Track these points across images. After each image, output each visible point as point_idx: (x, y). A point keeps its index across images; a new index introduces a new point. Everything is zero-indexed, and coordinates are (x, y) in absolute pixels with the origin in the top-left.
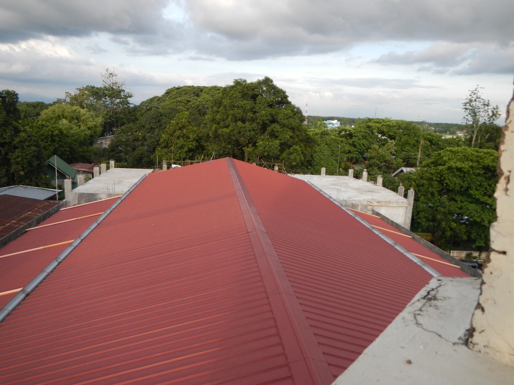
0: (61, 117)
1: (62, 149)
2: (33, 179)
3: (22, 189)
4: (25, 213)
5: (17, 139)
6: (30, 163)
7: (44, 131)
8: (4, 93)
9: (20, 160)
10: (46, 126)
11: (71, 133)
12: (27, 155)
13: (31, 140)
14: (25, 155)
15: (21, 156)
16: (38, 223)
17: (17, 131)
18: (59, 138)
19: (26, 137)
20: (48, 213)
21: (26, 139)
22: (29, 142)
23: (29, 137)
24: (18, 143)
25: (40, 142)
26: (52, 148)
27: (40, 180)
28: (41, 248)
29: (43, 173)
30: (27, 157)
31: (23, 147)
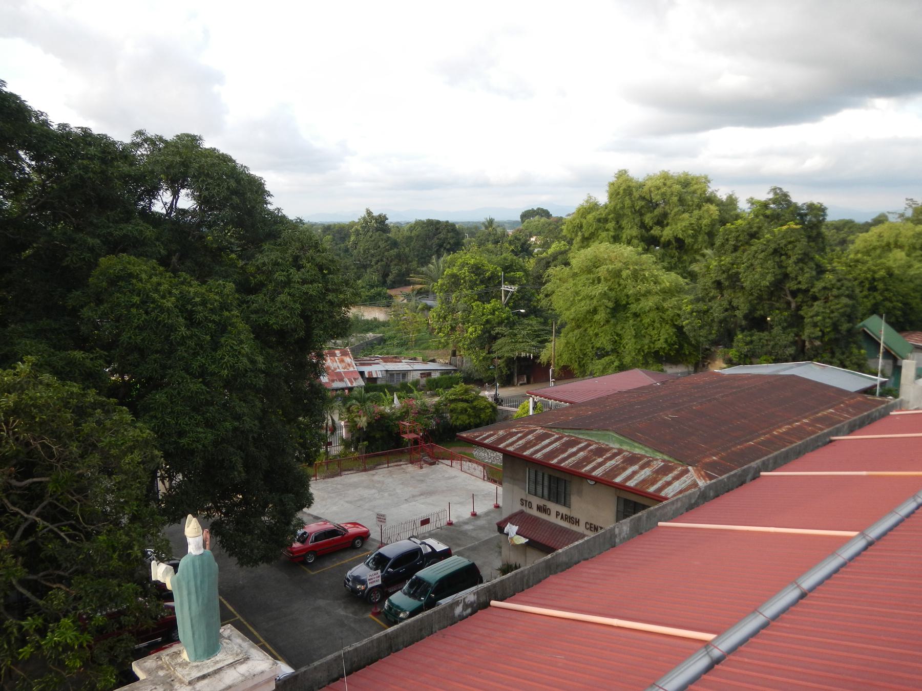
0: (892, 246)
1: (888, 304)
2: (837, 354)
3: (818, 368)
4: (823, 410)
5: (820, 285)
6: (835, 327)
7: (858, 272)
8: (805, 207)
9: (820, 320)
10: (863, 263)
11: (909, 275)
12: (832, 312)
13: (842, 286)
15: (823, 312)
16: (851, 431)
17: (821, 270)
18: (885, 284)
20: (868, 416)
21: (833, 286)
22: (839, 289)
23: (839, 280)
24: (820, 291)
25: (857, 290)
26: (870, 301)
27: (848, 357)
28: (864, 473)
29: (855, 345)
30: (832, 315)
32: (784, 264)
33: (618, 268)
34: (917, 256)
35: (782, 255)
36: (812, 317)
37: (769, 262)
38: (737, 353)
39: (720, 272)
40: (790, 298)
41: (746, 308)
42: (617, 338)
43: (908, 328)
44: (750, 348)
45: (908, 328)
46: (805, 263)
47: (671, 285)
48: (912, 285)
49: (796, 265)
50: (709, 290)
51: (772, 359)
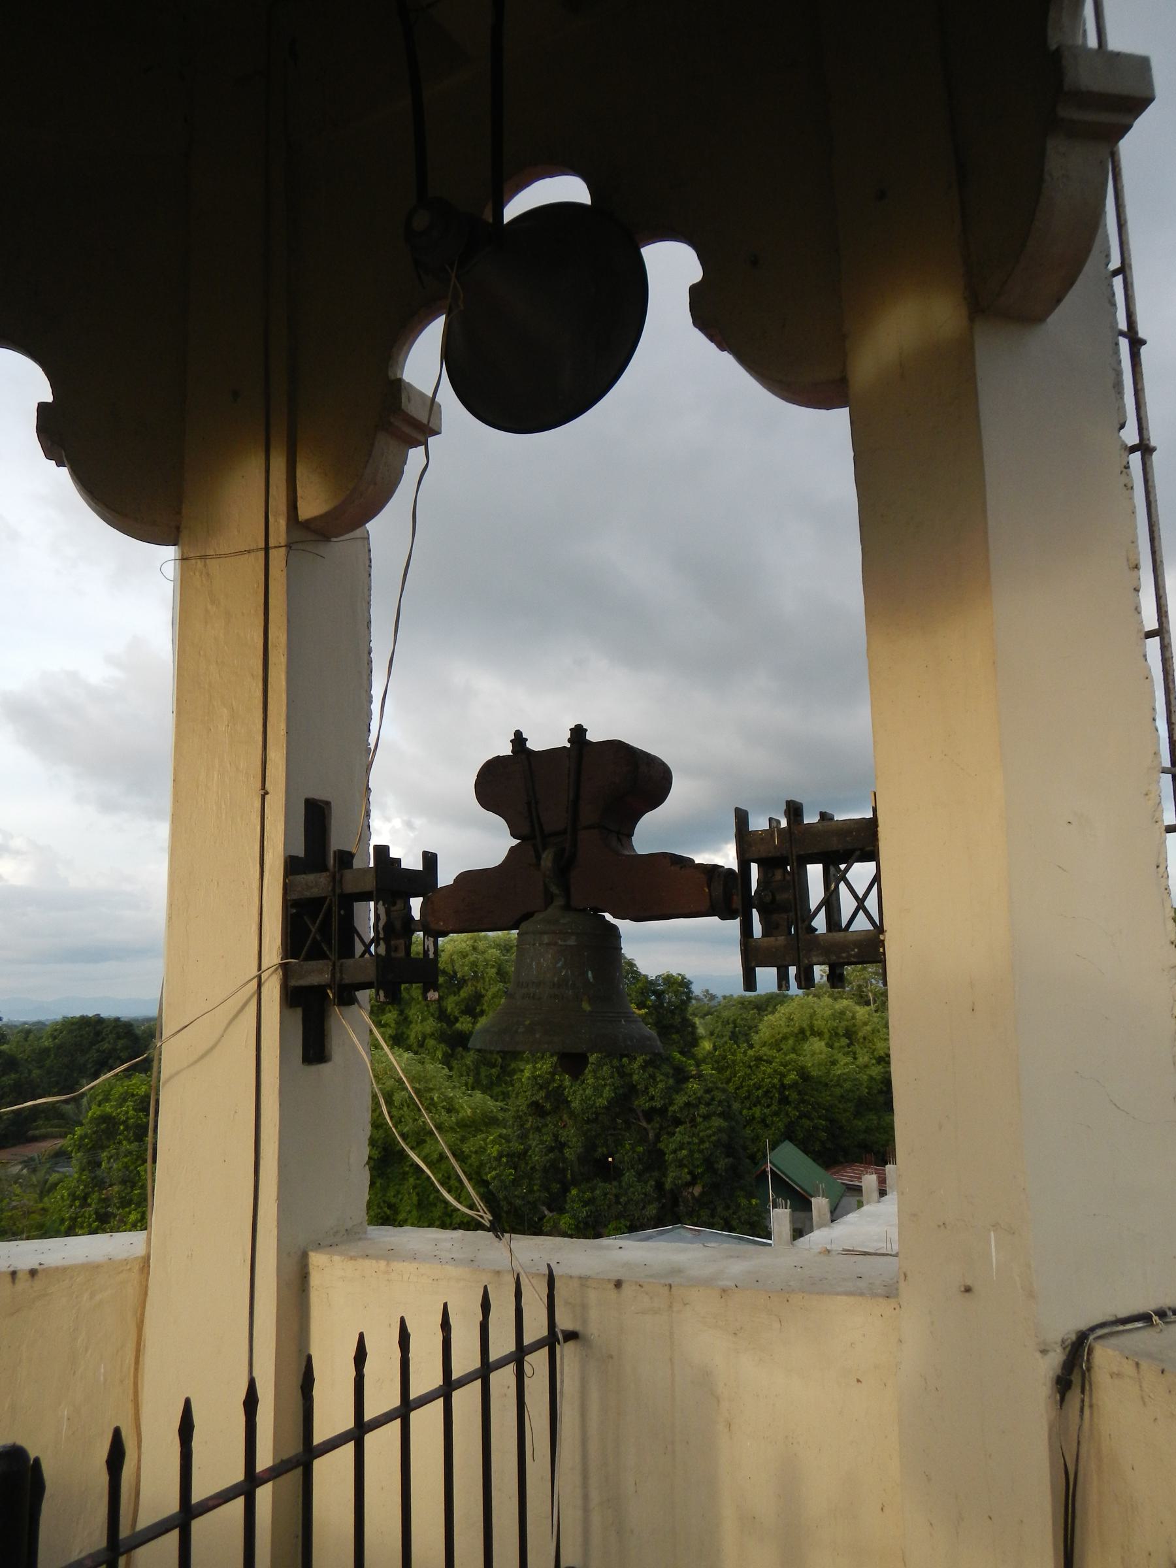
0: (808, 1033)
1: (806, 1123)
2: (719, 1209)
3: (689, 1235)
6: (709, 1164)
7: (761, 1076)
9: (686, 1156)
10: (767, 1061)
11: (834, 1075)
12: (702, 1141)
13: (713, 1099)
14: (697, 1141)
15: (689, 1143)
17: (681, 1076)
18: (799, 1093)
19: (702, 1091)
21: (700, 1099)
22: (708, 1104)
23: (708, 1091)
24: (681, 1109)
25: (736, 1106)
27: (734, 1213)
30: (702, 1147)
31: (693, 1120)
32: (628, 1071)
33: (388, 1089)
34: (843, 1047)
35: (622, 1056)
36: (675, 1152)
37: (605, 1068)
38: (572, 1222)
39: (536, 1088)
40: (644, 1124)
41: (579, 1144)
42: (388, 1212)
43: (842, 1159)
44: (591, 1212)
45: (842, 1159)
46: (658, 1067)
47: (474, 1112)
48: (838, 1091)
49: (644, 1071)
50: (524, 1118)
51: (626, 1227)
